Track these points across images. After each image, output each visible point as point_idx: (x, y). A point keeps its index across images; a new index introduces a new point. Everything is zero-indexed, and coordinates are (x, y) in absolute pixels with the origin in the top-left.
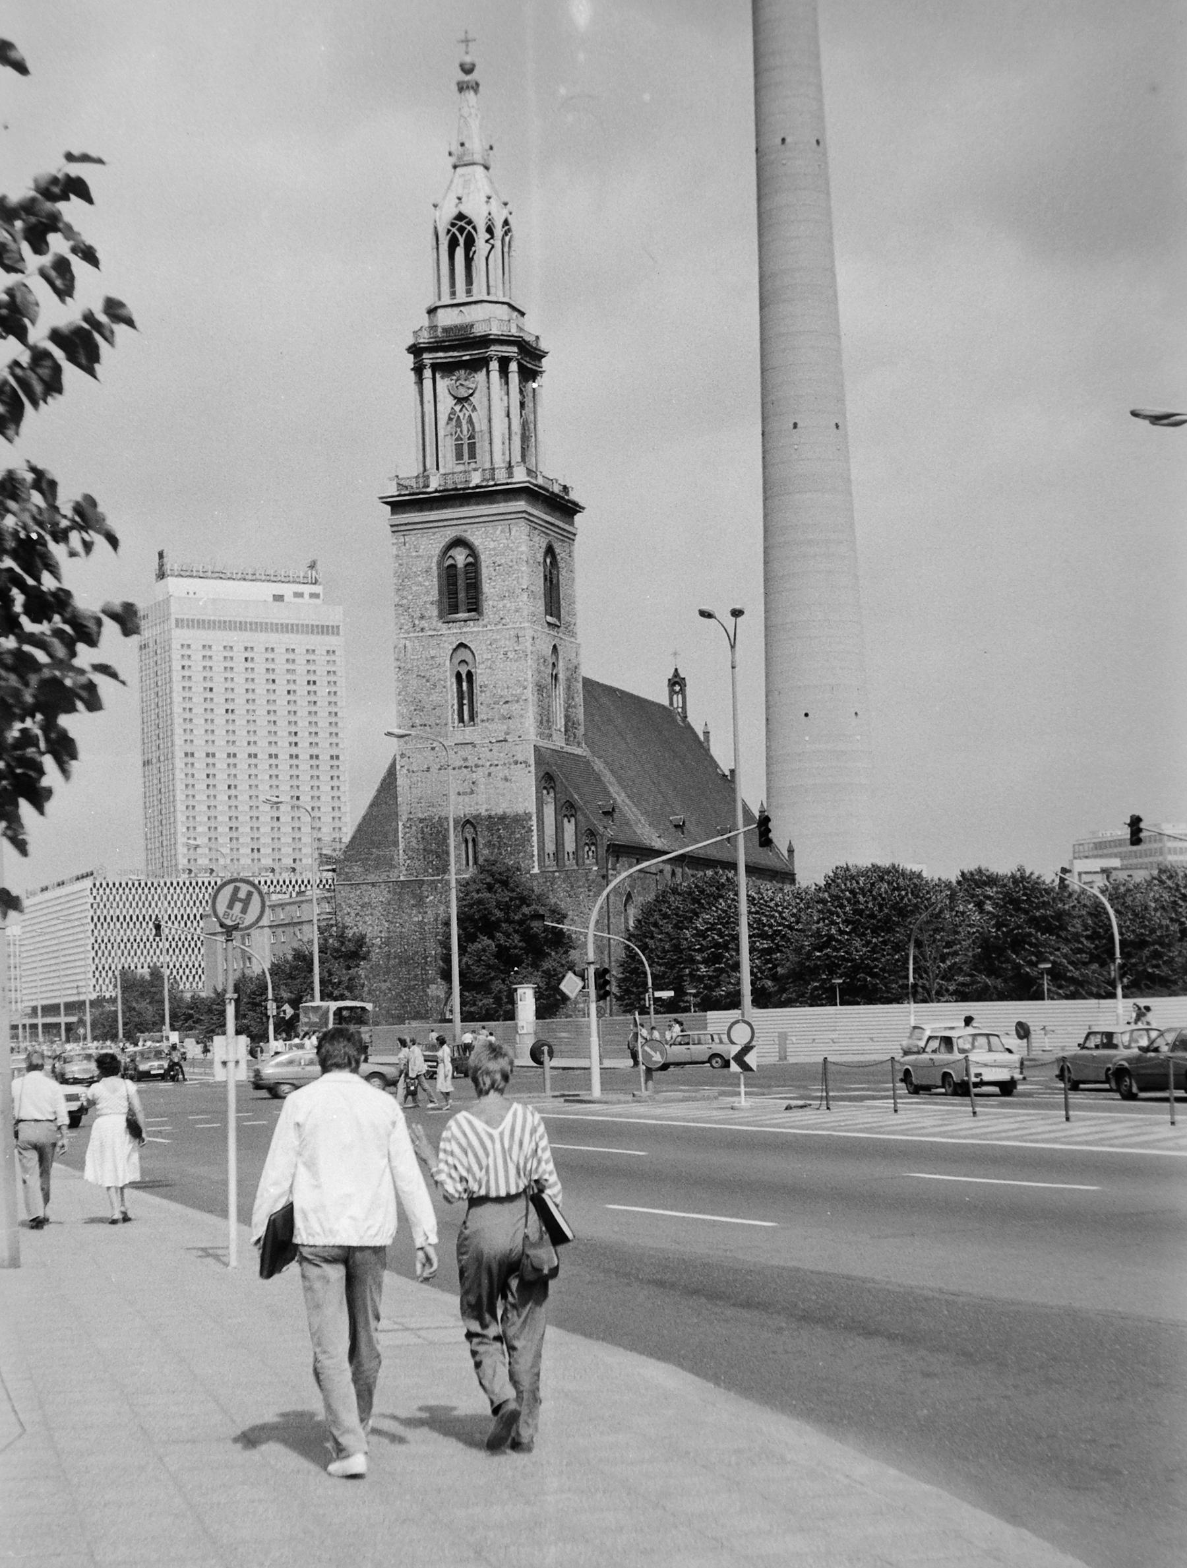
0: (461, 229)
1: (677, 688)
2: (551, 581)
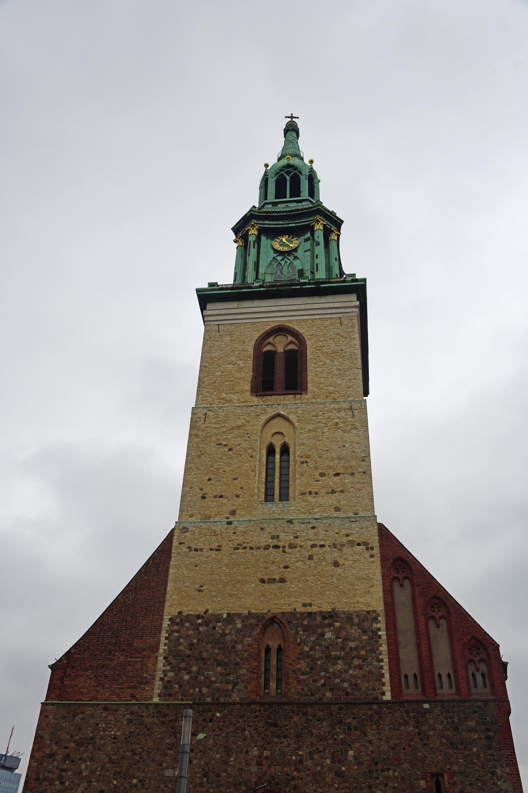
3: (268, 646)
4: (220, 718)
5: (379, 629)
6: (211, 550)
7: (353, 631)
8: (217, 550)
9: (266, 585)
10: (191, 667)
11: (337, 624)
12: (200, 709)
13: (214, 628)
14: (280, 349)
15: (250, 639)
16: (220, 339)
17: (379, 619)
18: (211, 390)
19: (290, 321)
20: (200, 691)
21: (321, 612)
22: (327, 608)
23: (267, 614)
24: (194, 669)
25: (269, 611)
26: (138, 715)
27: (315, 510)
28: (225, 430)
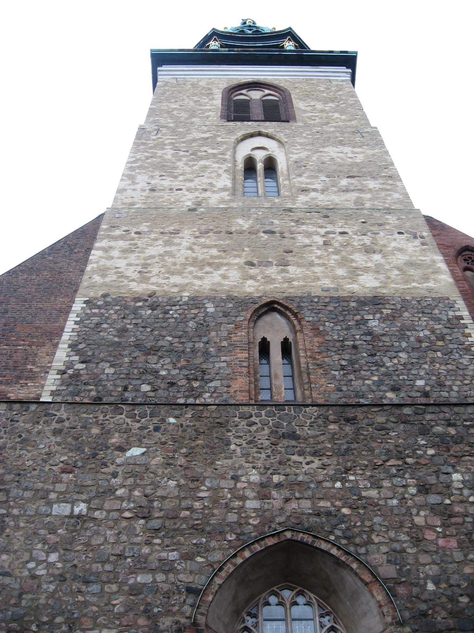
3: (264, 340)
4: (178, 426)
12: (136, 412)
23: (260, 297)
26: (7, 419)
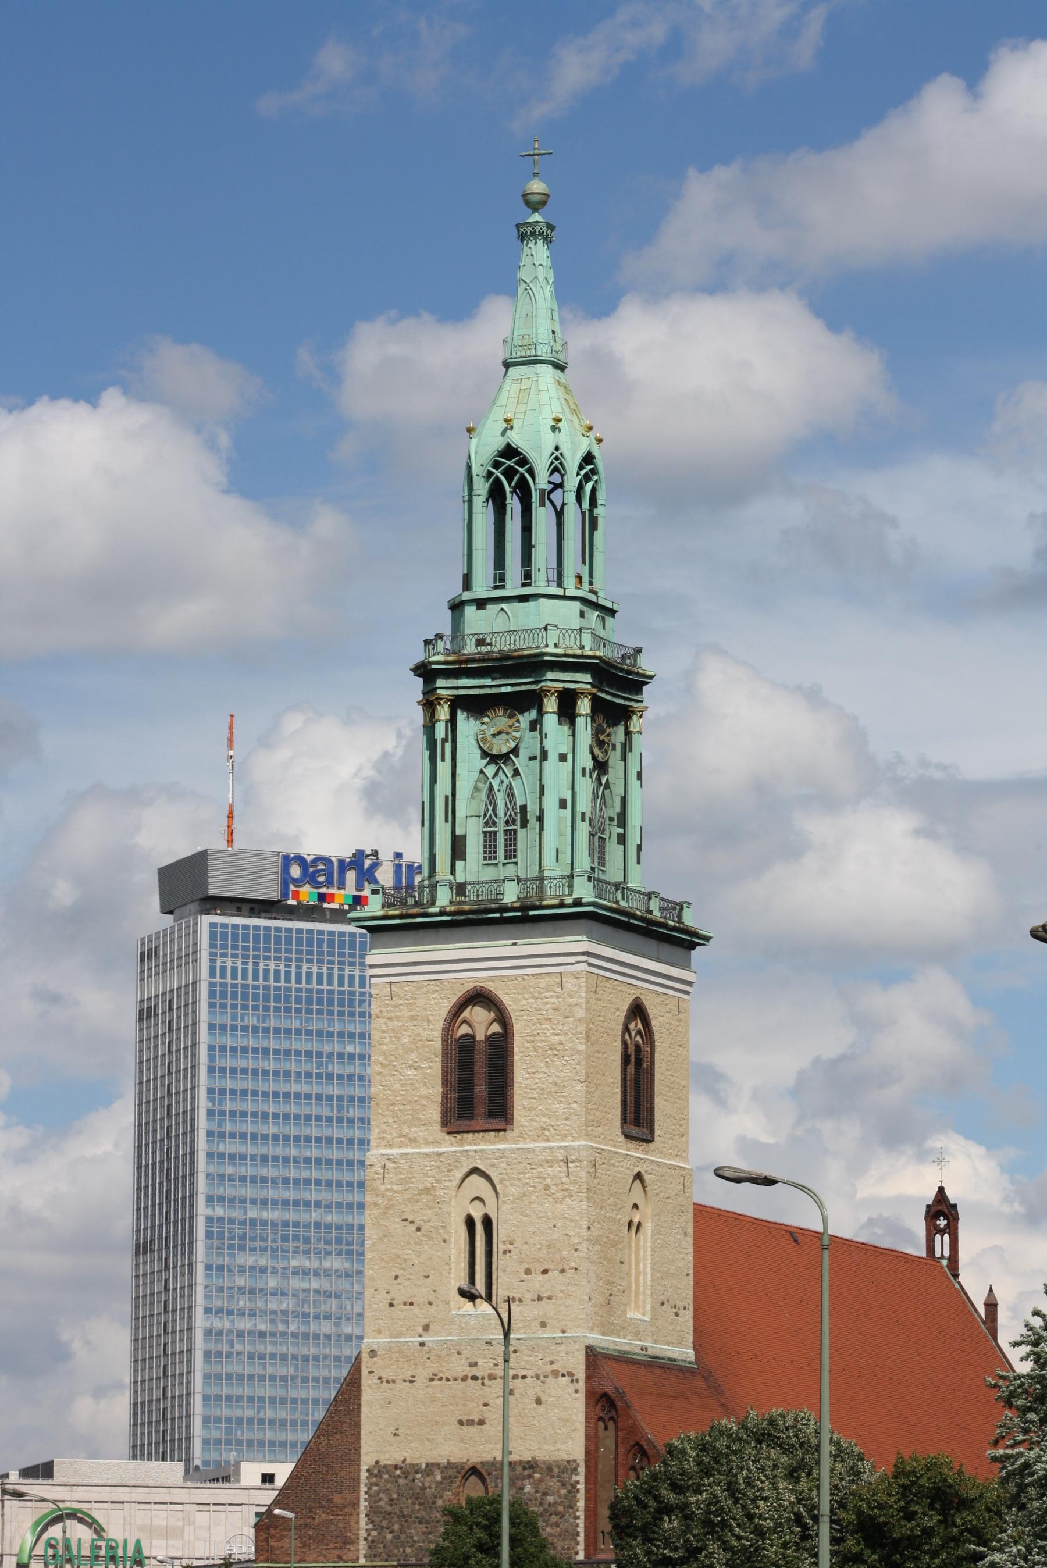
0: (509, 473)
1: (942, 1222)
2: (639, 1062)
5: (578, 1482)
6: (405, 1381)
7: (552, 1484)
8: (412, 1382)
9: (465, 1428)
10: (393, 1525)
11: (537, 1476)
13: (414, 1481)
14: (480, 1037)
15: (450, 1493)
16: (393, 1015)
17: (579, 1470)
18: (390, 1121)
19: (491, 979)
20: (404, 1552)
21: (521, 1462)
22: (527, 1457)
24: (396, 1527)
25: (468, 1460)
27: (520, 1325)
28: (410, 1196)
